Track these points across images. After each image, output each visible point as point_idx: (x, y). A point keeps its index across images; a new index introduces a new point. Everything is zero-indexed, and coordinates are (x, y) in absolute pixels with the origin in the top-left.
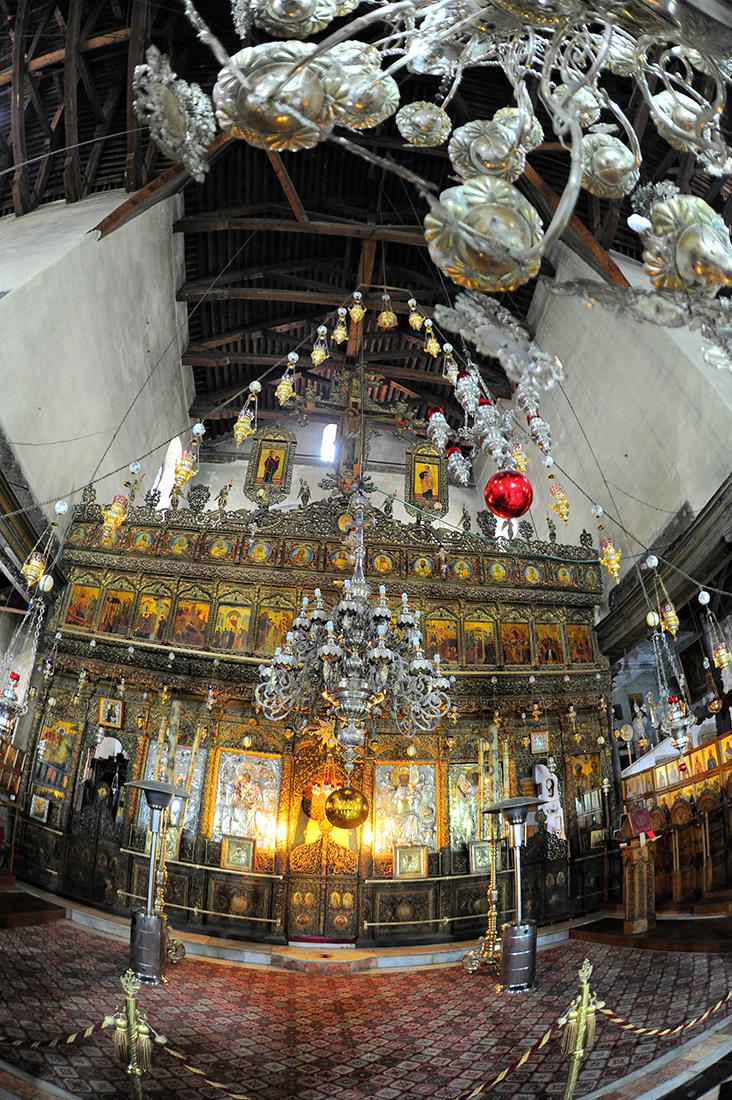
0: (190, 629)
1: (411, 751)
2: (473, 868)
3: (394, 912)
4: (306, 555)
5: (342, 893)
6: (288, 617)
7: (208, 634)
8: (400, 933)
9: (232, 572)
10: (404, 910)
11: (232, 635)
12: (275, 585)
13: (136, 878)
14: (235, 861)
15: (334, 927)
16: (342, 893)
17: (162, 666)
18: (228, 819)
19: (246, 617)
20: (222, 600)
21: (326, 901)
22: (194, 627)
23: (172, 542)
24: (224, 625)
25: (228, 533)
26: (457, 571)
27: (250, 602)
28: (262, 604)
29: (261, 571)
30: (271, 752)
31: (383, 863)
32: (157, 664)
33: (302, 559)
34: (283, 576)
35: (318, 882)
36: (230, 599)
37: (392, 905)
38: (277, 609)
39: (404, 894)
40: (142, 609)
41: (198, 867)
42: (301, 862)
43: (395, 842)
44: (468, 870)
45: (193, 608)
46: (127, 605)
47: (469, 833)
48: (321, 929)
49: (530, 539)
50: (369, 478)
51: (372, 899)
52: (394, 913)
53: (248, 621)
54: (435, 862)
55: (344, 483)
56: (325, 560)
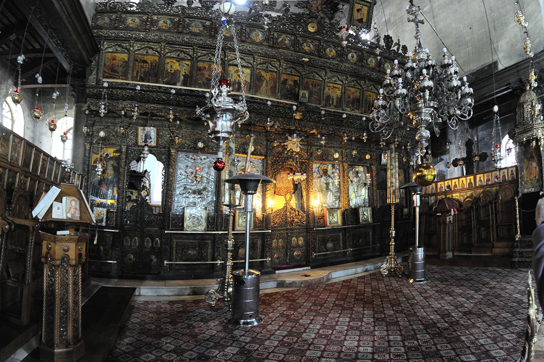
3: (325, 248)
6: (273, 76)
10: (330, 245)
12: (266, 55)
26: (369, 63)
35: (285, 232)
37: (324, 242)
38: (266, 71)
39: (329, 235)
40: (168, 67)
41: (220, 232)
46: (154, 64)
49: (406, 55)
52: (325, 248)
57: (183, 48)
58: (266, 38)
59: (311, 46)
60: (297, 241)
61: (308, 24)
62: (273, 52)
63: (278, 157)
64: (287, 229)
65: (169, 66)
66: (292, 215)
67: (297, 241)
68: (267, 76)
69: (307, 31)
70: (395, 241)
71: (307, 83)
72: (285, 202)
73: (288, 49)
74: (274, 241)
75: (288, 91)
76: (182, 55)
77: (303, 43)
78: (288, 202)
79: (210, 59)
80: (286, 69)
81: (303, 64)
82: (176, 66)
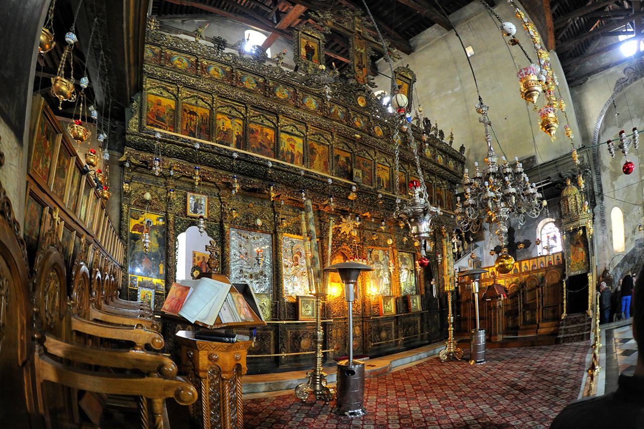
9: (291, 110)
12: (320, 126)
27: (302, 135)
34: (326, 123)
36: (289, 129)
40: (220, 123)
45: (262, 130)
53: (302, 147)
57: (235, 105)
59: (361, 122)
62: (326, 123)
68: (319, 149)
70: (453, 327)
73: (341, 122)
76: (234, 113)
79: (262, 121)
80: (338, 143)
81: (354, 140)
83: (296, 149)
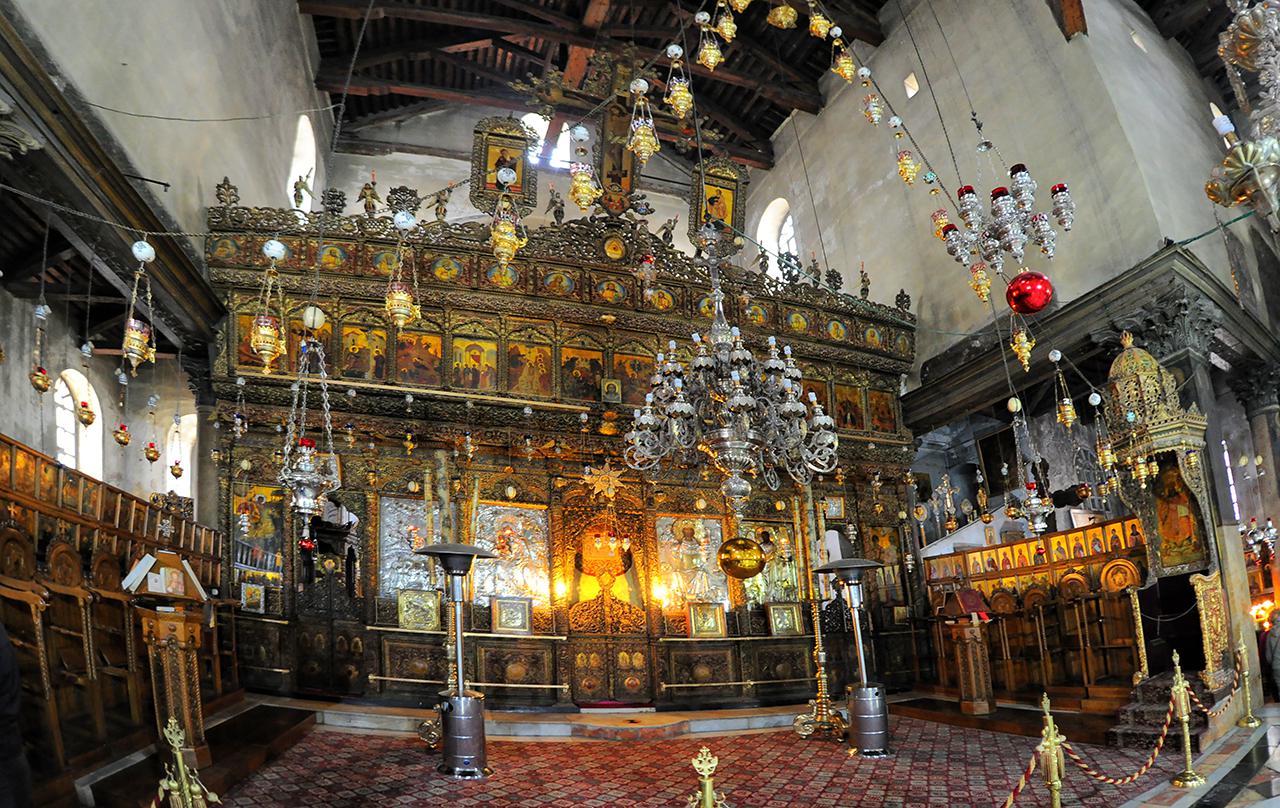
0: (418, 365)
1: (701, 504)
2: (774, 631)
3: (692, 673)
4: (565, 283)
5: (631, 652)
7: (443, 369)
8: (699, 696)
9: (465, 297)
10: (702, 671)
11: (476, 372)
13: (387, 657)
14: (511, 625)
15: (624, 690)
16: (631, 652)
17: (388, 410)
18: (491, 577)
19: (490, 352)
20: (456, 331)
21: (614, 661)
22: (424, 363)
23: (374, 259)
24: (465, 361)
25: (456, 251)
27: (494, 335)
28: (511, 337)
29: (507, 300)
30: (534, 503)
31: (673, 621)
32: (381, 408)
33: (561, 288)
34: (538, 306)
36: (468, 330)
38: (531, 344)
39: (700, 653)
40: (348, 343)
42: (582, 620)
43: (684, 599)
44: (768, 632)
45: (419, 340)
47: (762, 594)
48: (612, 693)
50: (644, 197)
51: (667, 658)
53: (495, 357)
54: (733, 620)
55: (610, 200)
56: (590, 290)
57: (370, 306)
58: (520, 277)
59: (618, 288)
60: (631, 659)
61: (605, 242)
63: (577, 506)
64: (606, 638)
65: (350, 340)
66: (615, 613)
67: (631, 659)
68: (531, 355)
69: (604, 257)
70: (826, 672)
71: (620, 364)
72: (600, 589)
74: (580, 656)
75: (579, 382)
76: (370, 319)
77: (600, 284)
78: (606, 588)
79: (419, 325)
80: (569, 339)
81: (604, 327)
82: (362, 340)
83: (484, 362)
